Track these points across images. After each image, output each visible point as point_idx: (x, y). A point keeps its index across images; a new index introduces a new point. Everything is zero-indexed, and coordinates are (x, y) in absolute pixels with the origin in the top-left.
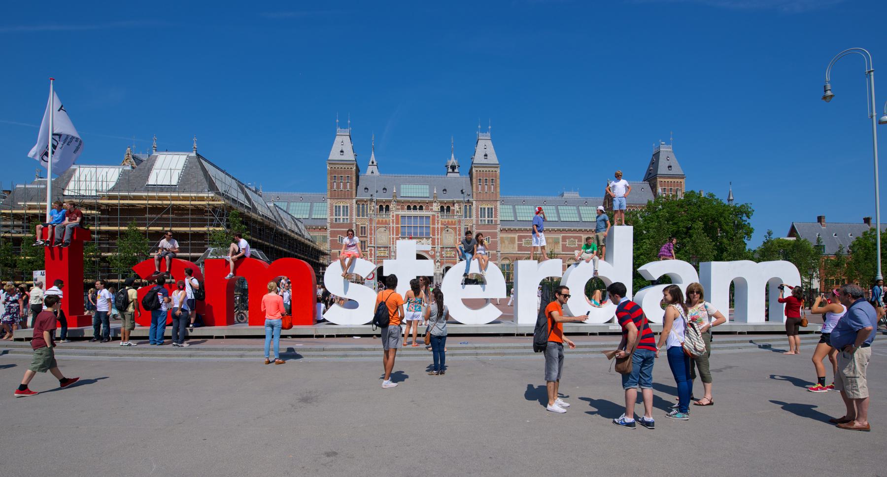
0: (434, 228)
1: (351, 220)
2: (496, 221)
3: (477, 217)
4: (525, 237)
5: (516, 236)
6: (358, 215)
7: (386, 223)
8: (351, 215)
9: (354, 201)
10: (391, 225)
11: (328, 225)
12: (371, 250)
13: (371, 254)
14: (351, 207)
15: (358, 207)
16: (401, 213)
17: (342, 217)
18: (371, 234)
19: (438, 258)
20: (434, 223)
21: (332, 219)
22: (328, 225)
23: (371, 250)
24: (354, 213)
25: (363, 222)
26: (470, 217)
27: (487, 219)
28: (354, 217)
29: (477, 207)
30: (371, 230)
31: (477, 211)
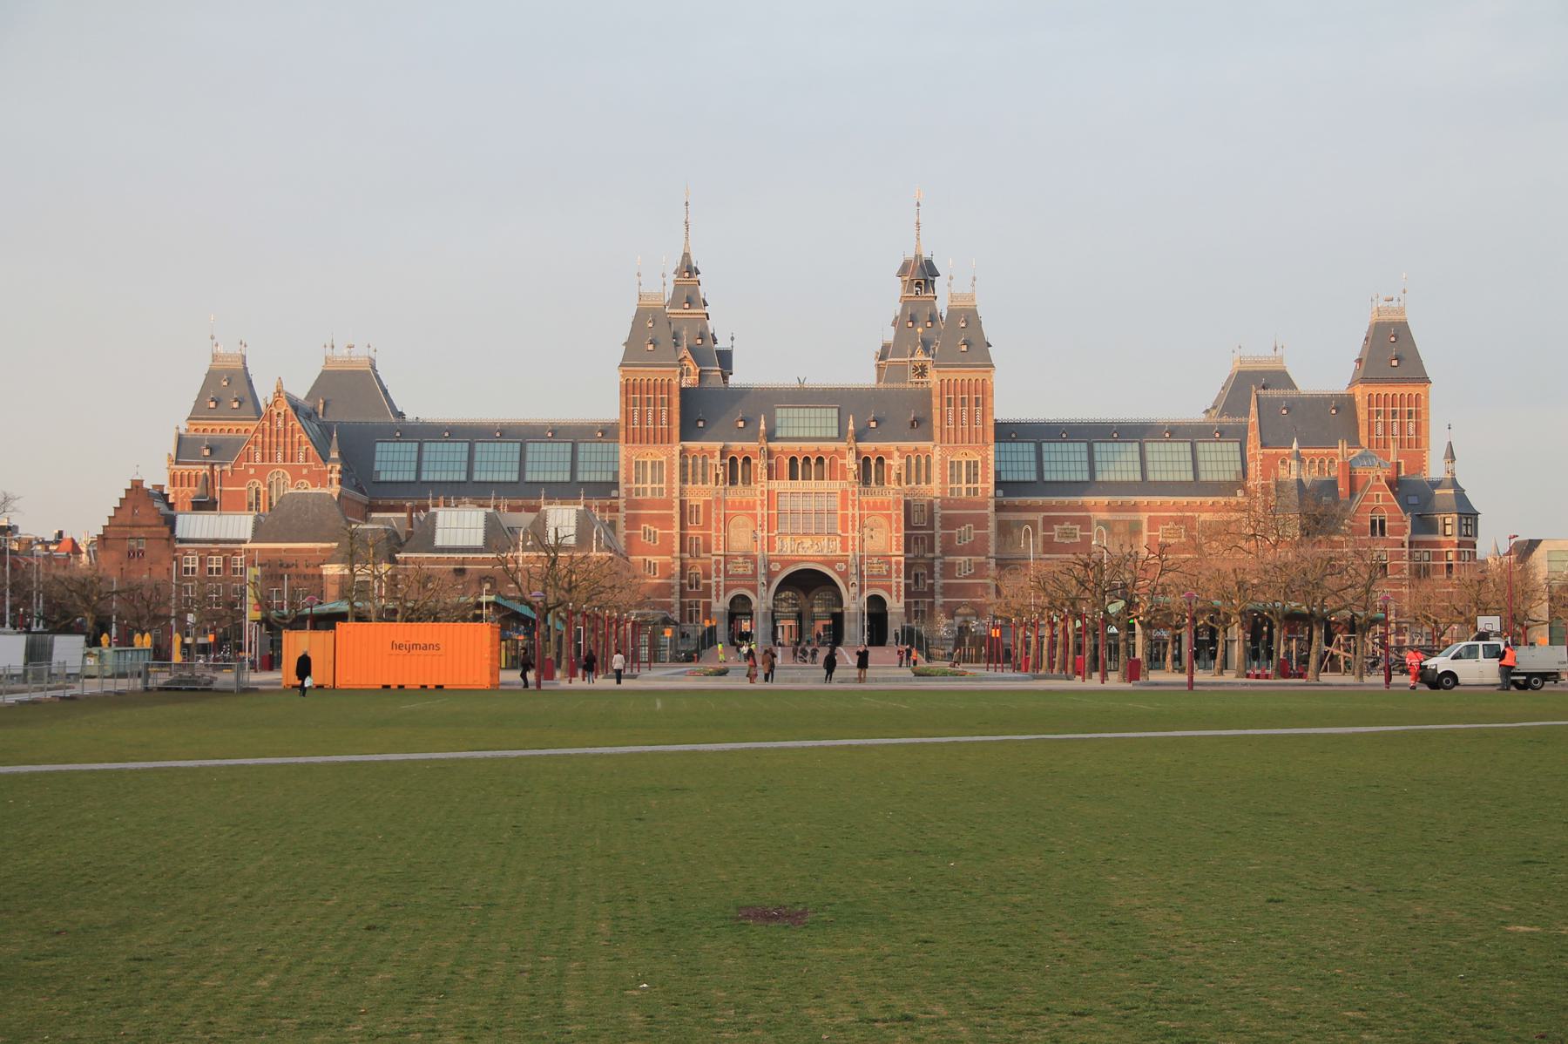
0: (844, 517)
1: (670, 491)
2: (985, 490)
3: (943, 481)
4: (1060, 520)
5: (1039, 517)
6: (684, 480)
7: (750, 506)
8: (670, 480)
9: (677, 453)
10: (759, 511)
11: (621, 503)
12: (718, 562)
13: (718, 571)
14: (670, 464)
15: (683, 466)
16: (776, 485)
17: (648, 485)
18: (718, 530)
19: (854, 579)
20: (844, 507)
21: (629, 491)
22: (621, 503)
23: (718, 562)
24: (677, 475)
25: (698, 494)
26: (928, 481)
27: (964, 485)
28: (677, 484)
29: (943, 460)
30: (718, 521)
31: (943, 468)
